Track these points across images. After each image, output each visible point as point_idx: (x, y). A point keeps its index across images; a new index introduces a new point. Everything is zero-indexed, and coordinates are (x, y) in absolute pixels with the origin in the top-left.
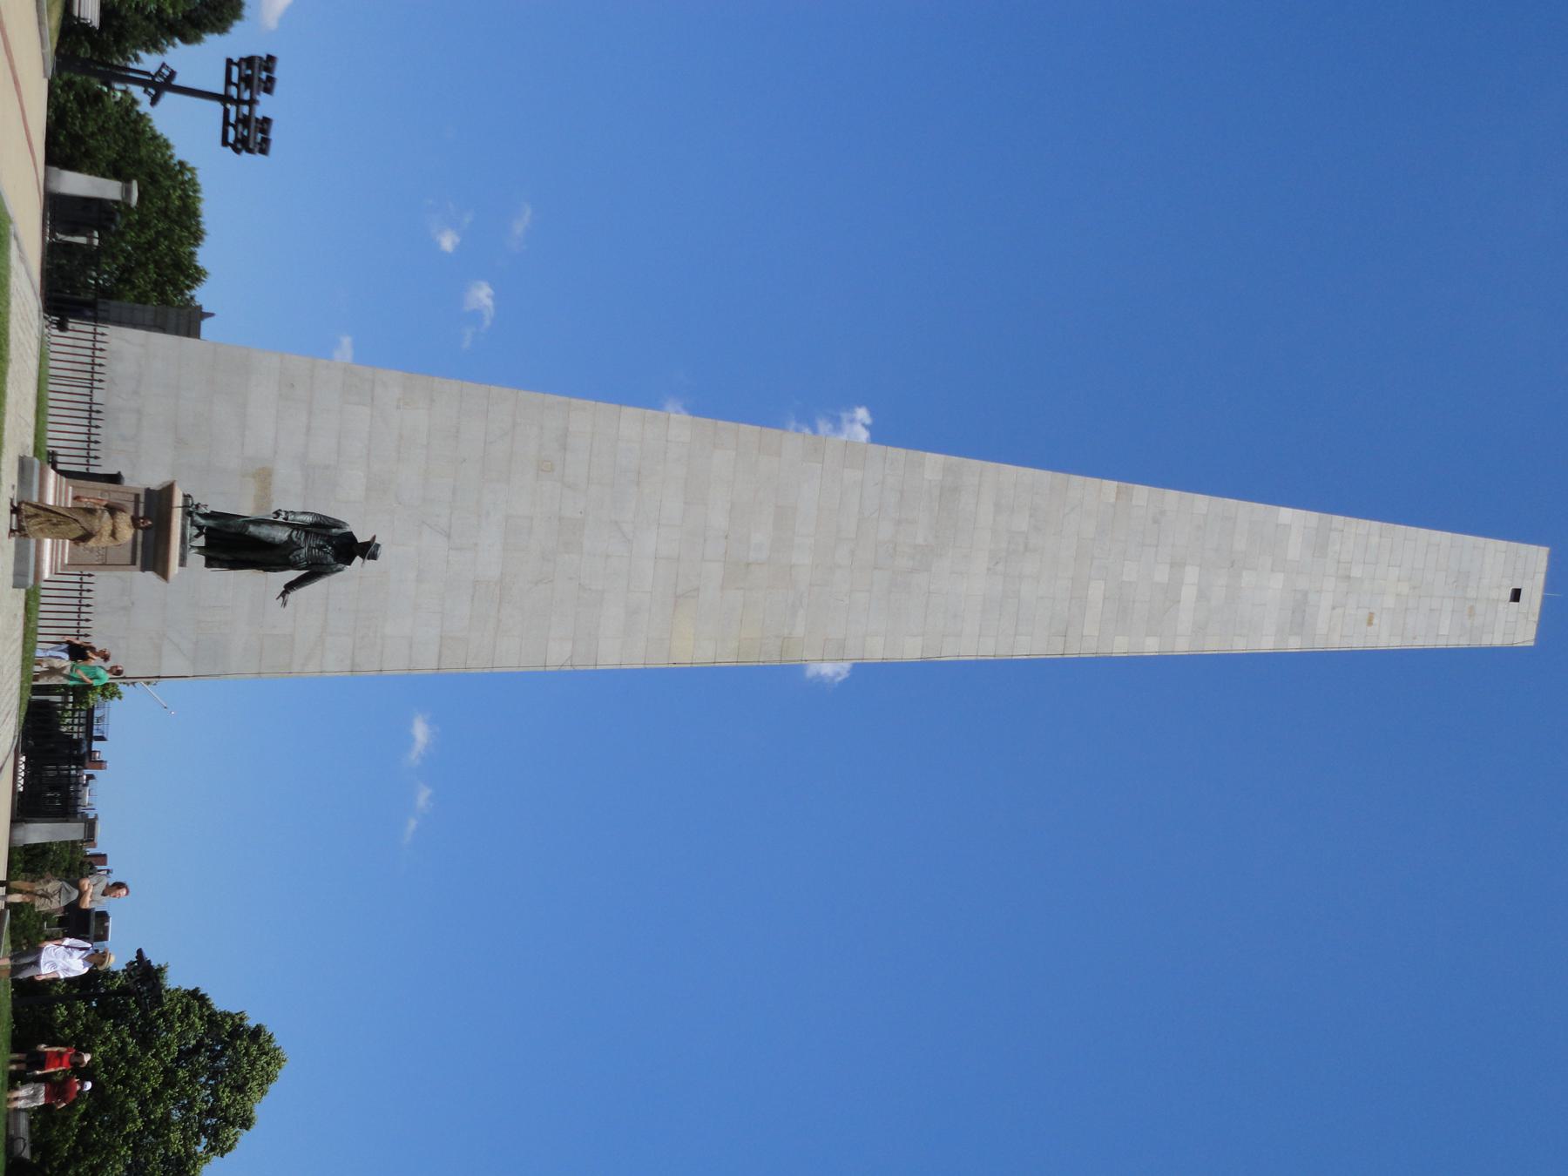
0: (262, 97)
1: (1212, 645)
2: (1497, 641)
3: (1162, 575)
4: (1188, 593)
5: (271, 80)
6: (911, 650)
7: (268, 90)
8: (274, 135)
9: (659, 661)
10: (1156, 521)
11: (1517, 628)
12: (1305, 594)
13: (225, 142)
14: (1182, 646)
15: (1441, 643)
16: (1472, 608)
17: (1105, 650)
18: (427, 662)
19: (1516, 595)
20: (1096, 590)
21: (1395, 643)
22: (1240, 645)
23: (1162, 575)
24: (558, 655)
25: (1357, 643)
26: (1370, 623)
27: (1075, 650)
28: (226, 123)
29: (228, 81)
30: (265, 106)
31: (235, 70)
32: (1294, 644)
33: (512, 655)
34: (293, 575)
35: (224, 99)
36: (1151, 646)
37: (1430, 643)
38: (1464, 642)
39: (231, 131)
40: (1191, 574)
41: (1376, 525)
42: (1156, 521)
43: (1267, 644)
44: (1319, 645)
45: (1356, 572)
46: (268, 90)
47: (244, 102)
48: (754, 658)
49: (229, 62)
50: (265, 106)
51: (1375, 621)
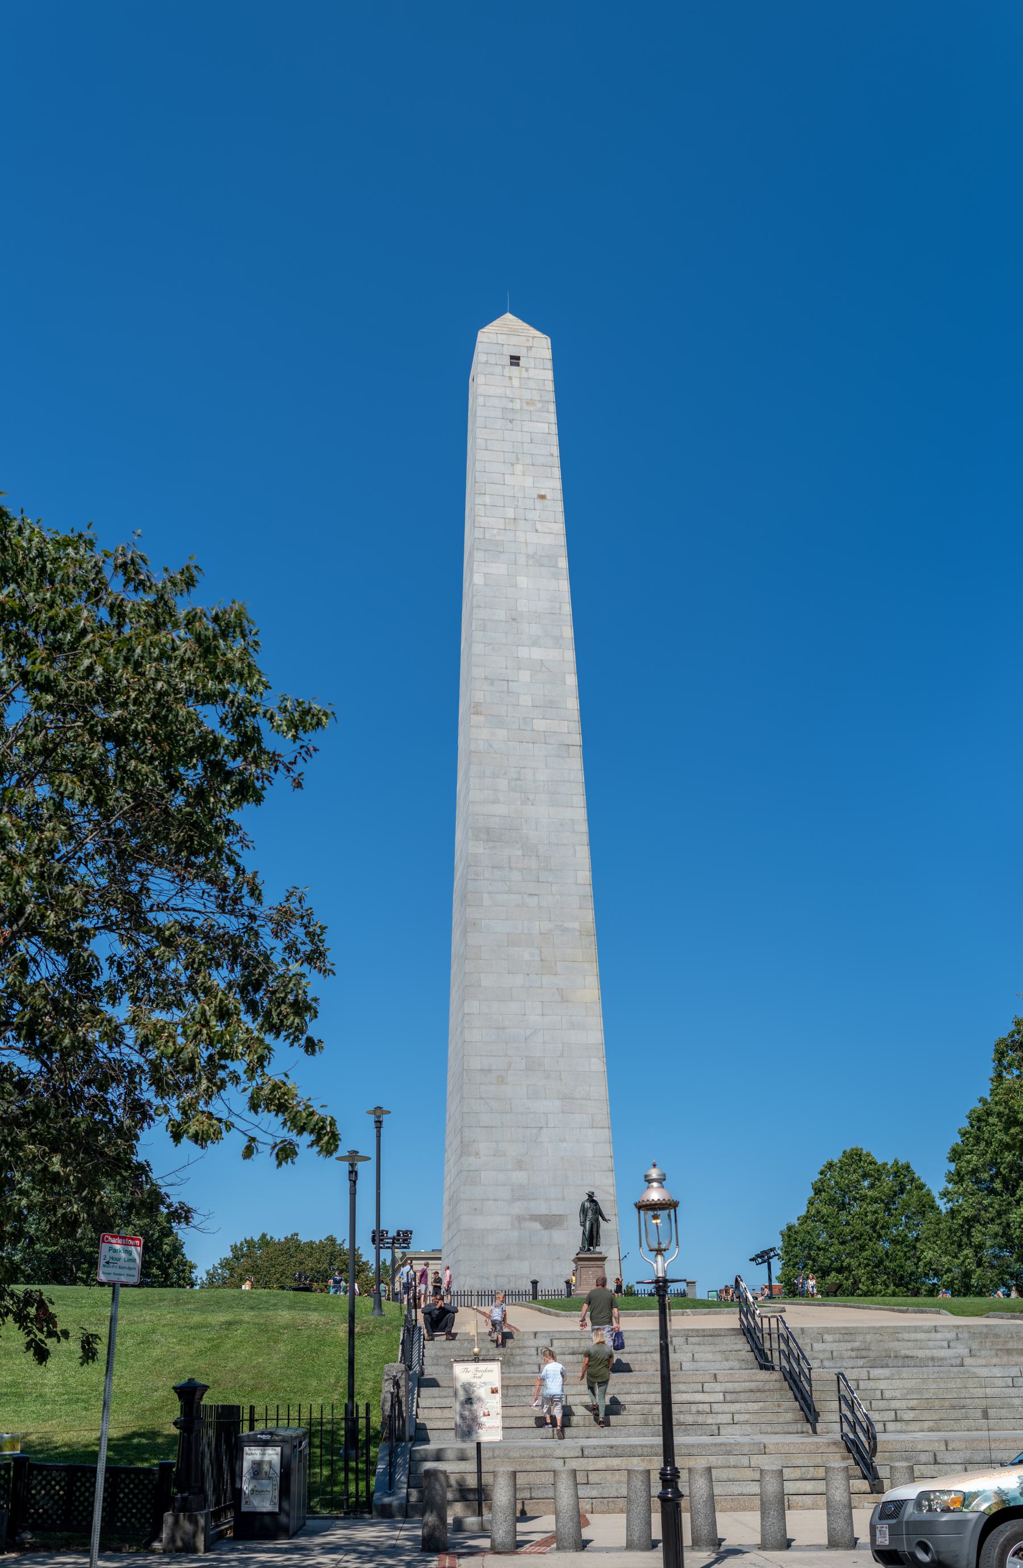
1: (568, 632)
2: (549, 375)
3: (525, 676)
4: (537, 653)
6: (583, 854)
9: (598, 1009)
10: (492, 684)
11: (538, 347)
12: (528, 556)
14: (570, 655)
15: (554, 429)
16: (527, 403)
17: (576, 715)
18: (606, 1134)
19: (515, 360)
20: (540, 725)
21: (557, 472)
22: (567, 609)
23: (525, 676)
24: (598, 1065)
25: (559, 507)
26: (542, 497)
27: (577, 739)
32: (563, 563)
33: (598, 1089)
36: (572, 680)
37: (555, 440)
38: (552, 408)
40: (524, 652)
42: (492, 684)
43: (565, 586)
44: (562, 540)
45: (510, 513)
48: (593, 952)
51: (543, 493)
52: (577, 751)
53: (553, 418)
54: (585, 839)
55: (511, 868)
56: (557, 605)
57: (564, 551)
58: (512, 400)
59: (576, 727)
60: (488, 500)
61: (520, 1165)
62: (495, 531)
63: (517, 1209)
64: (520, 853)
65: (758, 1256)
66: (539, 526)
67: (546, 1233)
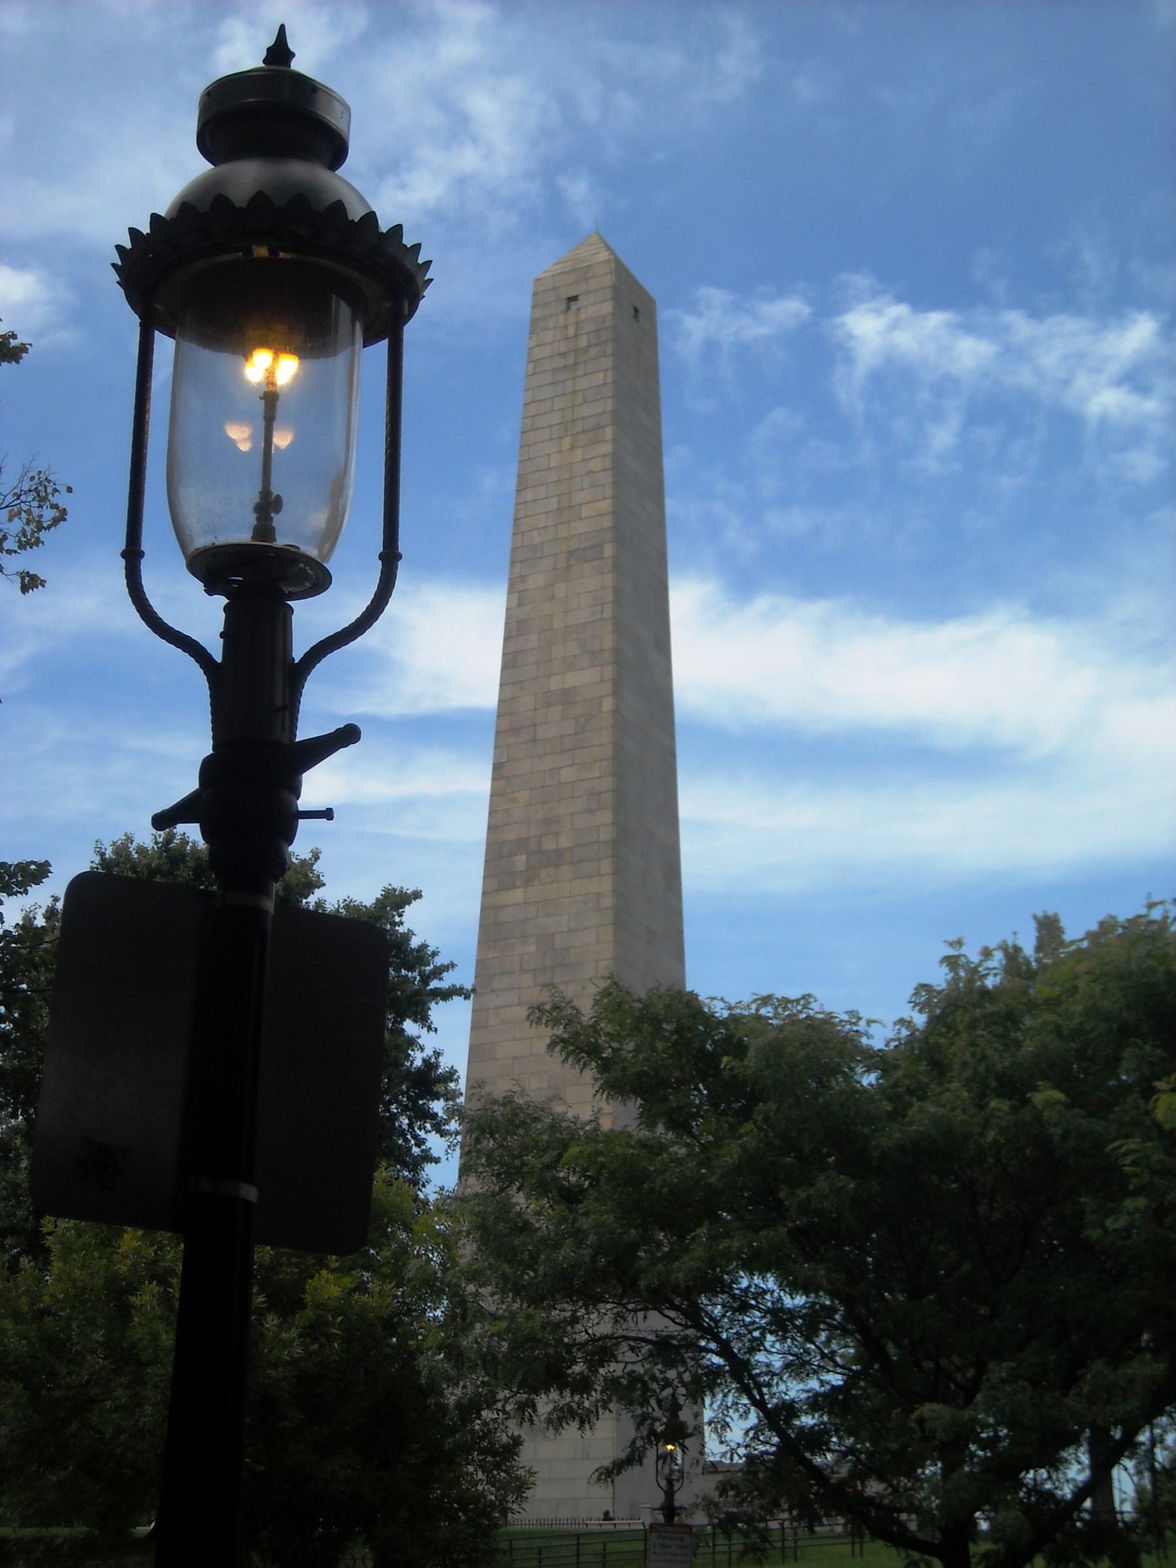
4: (572, 680)
40: (555, 684)
58: (564, 355)
62: (535, 533)
64: (532, 948)
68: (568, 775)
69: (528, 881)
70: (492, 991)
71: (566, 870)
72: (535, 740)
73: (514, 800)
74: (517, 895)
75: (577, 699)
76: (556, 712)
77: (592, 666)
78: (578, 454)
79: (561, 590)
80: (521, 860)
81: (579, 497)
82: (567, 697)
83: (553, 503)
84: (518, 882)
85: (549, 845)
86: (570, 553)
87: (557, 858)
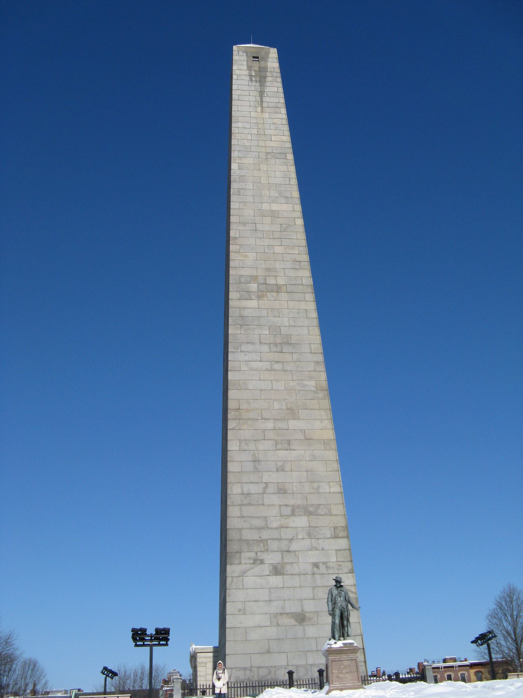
0: (148, 632)
1: (296, 194)
4: (275, 207)
5: (141, 630)
7: (145, 630)
8: (161, 627)
13: (167, 645)
15: (281, 90)
27: (306, 257)
28: (159, 645)
29: (144, 645)
30: (151, 631)
31: (138, 643)
32: (290, 157)
34: (349, 605)
35: (151, 646)
37: (282, 95)
38: (279, 80)
39: (161, 643)
40: (265, 207)
41: (233, 125)
43: (293, 169)
44: (289, 145)
46: (145, 630)
47: (151, 638)
49: (136, 645)
50: (151, 631)
52: (307, 265)
53: (280, 85)
54: (316, 322)
55: (260, 343)
56: (288, 179)
57: (291, 151)
59: (304, 250)
60: (240, 125)
61: (277, 570)
62: (245, 141)
63: (274, 608)
64: (267, 332)
65: (477, 639)
66: (273, 138)
67: (300, 629)
68: (279, 250)
69: (259, 297)
70: (241, 351)
71: (283, 296)
72: (256, 230)
73: (246, 256)
74: (254, 303)
75: (280, 216)
76: (267, 220)
77: (287, 203)
78: (266, 115)
79: (264, 167)
80: (254, 287)
81: (268, 132)
82: (274, 215)
83: (255, 131)
84: (253, 297)
85: (271, 281)
86: (267, 153)
87: (278, 289)
